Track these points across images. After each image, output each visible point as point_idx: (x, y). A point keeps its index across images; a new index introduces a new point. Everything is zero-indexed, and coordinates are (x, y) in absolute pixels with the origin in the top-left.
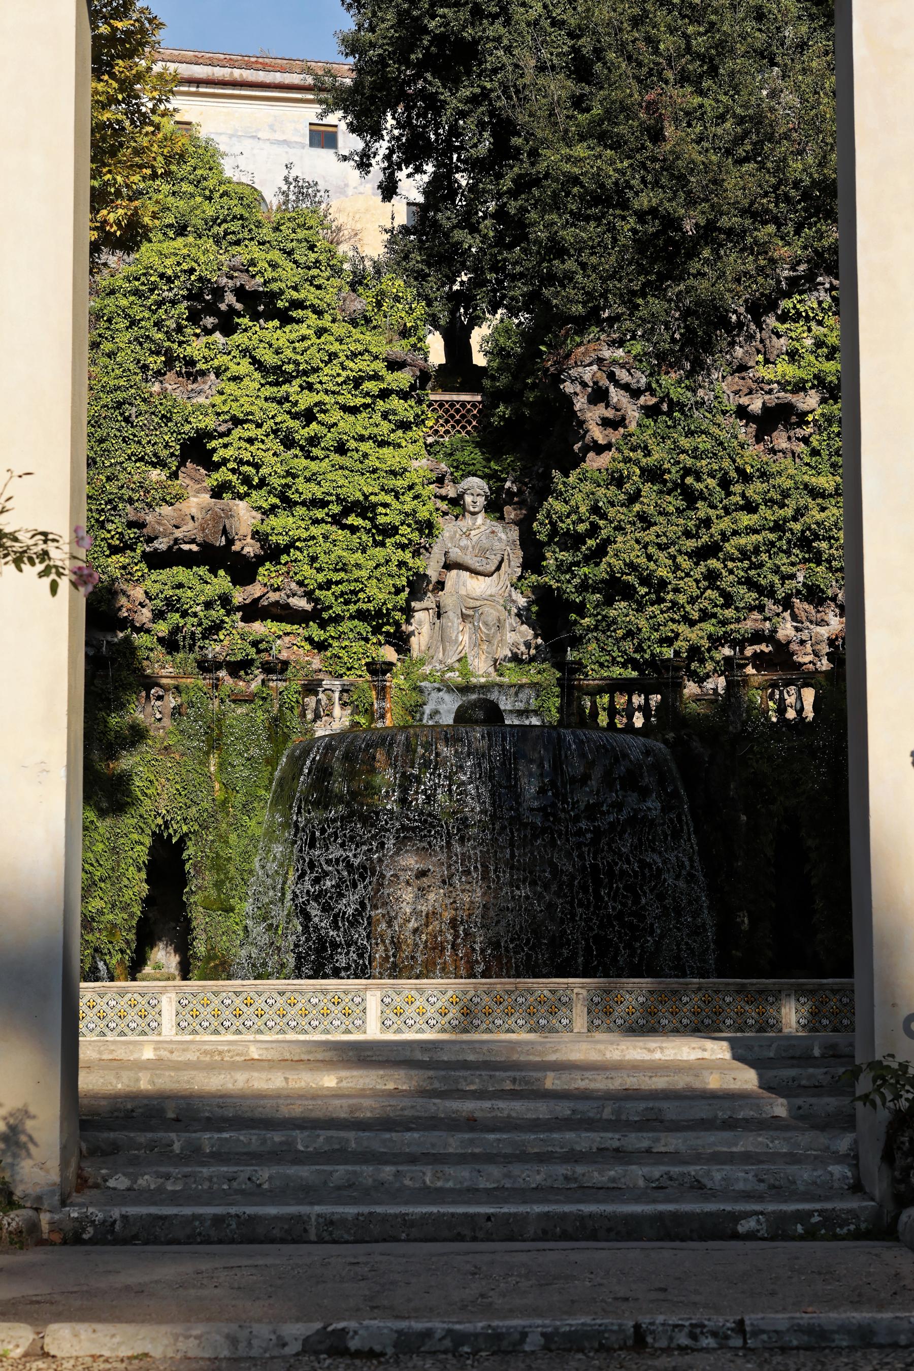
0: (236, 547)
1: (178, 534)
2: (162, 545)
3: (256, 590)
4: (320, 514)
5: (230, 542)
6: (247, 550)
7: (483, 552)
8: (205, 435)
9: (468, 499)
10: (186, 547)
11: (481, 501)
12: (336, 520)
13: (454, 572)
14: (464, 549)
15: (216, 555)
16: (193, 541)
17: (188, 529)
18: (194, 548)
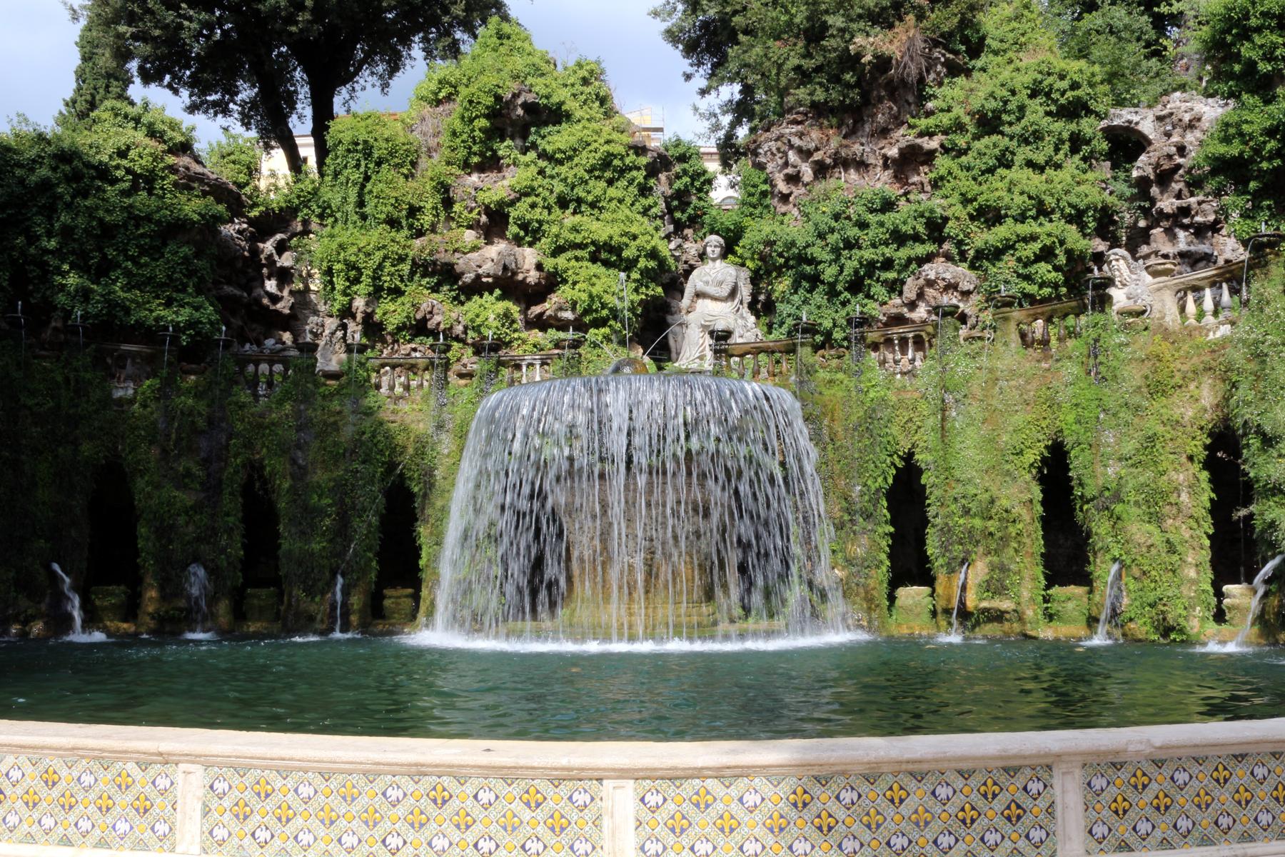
0: (520, 277)
1: (480, 271)
2: (468, 278)
3: (536, 310)
4: (579, 253)
5: (515, 273)
6: (528, 280)
7: (720, 283)
8: (501, 204)
9: (709, 250)
10: (484, 280)
11: (718, 250)
12: (594, 259)
13: (700, 301)
14: (707, 283)
15: (507, 284)
16: (488, 276)
17: (488, 267)
18: (490, 280)
